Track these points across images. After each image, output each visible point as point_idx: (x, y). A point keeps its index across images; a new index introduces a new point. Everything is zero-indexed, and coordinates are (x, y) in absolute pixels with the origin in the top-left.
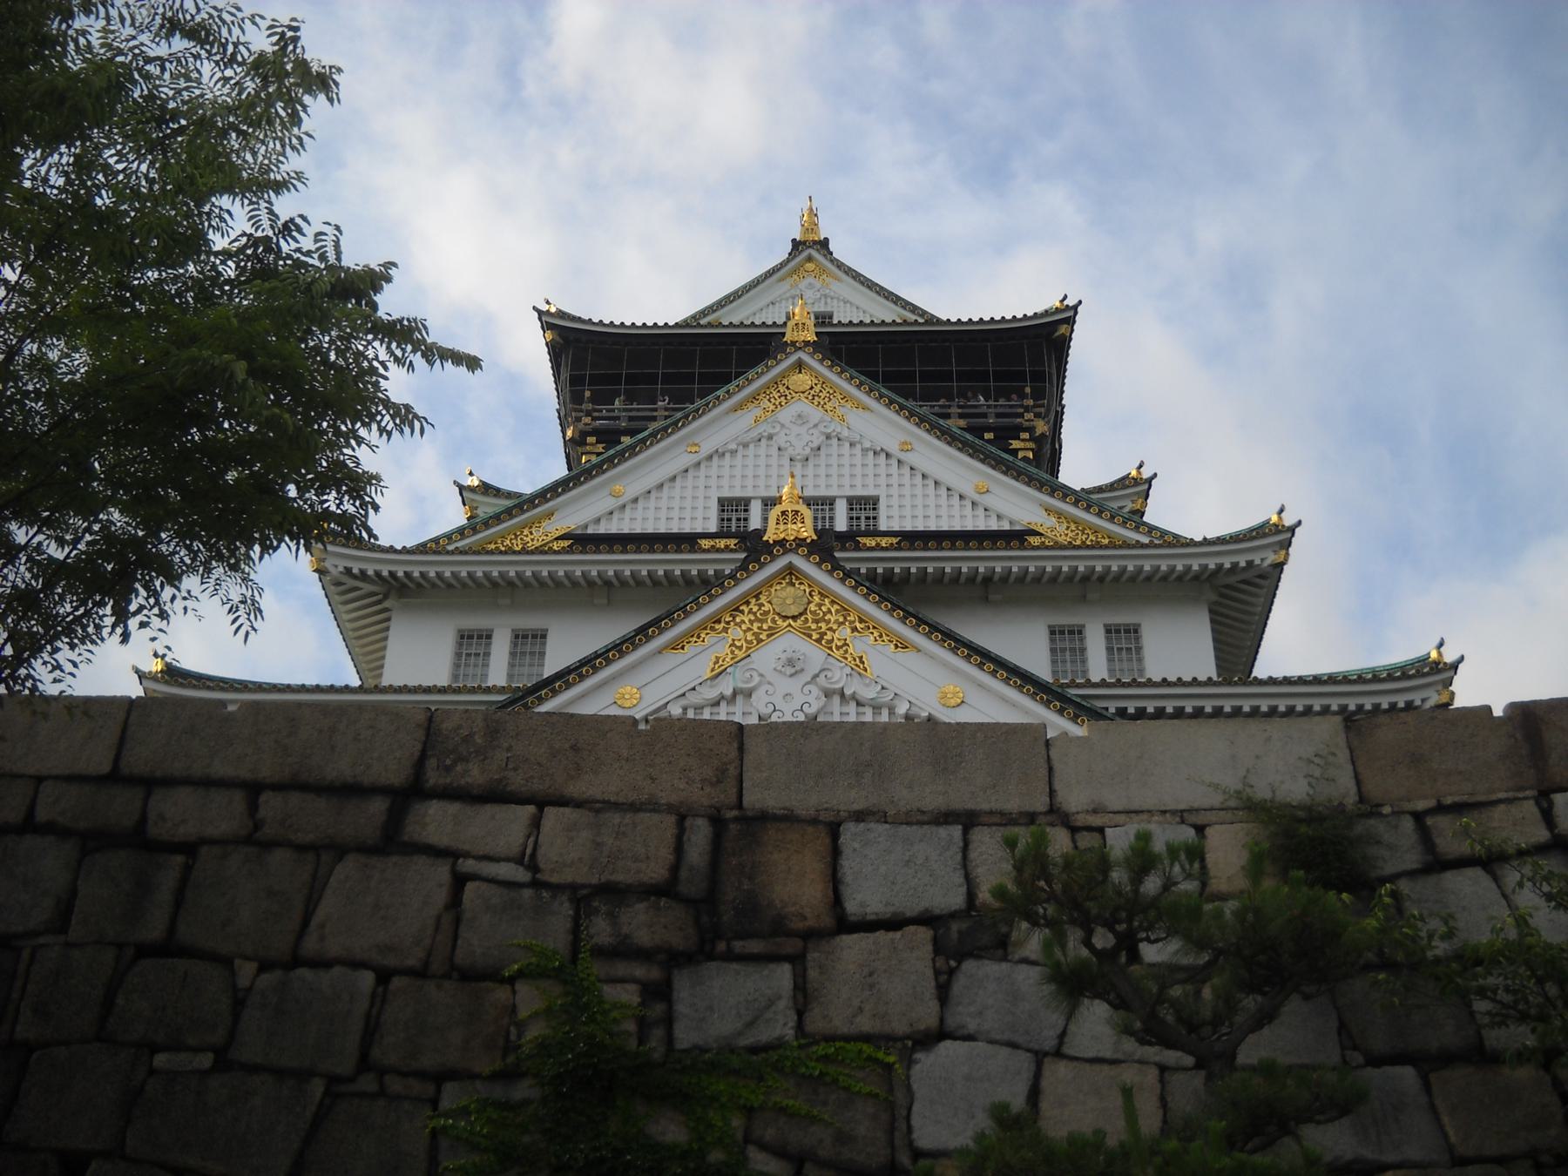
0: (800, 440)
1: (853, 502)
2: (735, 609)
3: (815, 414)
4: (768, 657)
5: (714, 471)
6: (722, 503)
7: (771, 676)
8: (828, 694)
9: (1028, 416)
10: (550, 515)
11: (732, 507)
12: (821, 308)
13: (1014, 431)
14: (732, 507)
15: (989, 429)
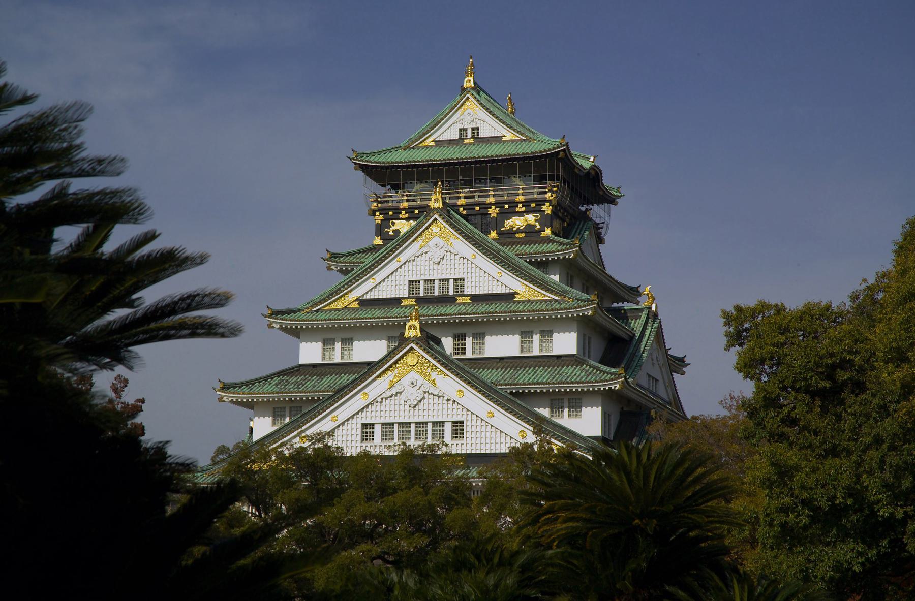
0: (436, 254)
1: (455, 280)
2: (396, 362)
3: (441, 242)
4: (406, 381)
5: (406, 268)
6: (410, 282)
7: (407, 387)
8: (425, 392)
9: (549, 194)
10: (350, 291)
11: (413, 283)
12: (474, 126)
13: (544, 201)
14: (413, 283)
15: (533, 202)
